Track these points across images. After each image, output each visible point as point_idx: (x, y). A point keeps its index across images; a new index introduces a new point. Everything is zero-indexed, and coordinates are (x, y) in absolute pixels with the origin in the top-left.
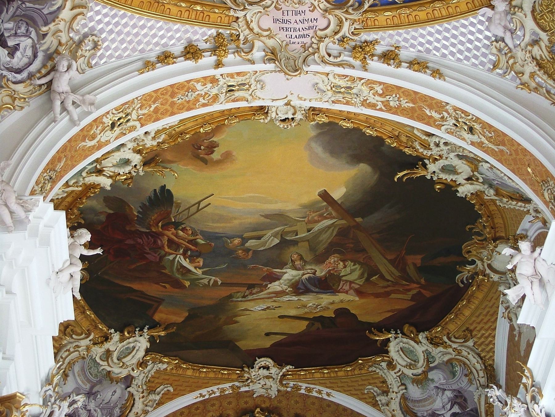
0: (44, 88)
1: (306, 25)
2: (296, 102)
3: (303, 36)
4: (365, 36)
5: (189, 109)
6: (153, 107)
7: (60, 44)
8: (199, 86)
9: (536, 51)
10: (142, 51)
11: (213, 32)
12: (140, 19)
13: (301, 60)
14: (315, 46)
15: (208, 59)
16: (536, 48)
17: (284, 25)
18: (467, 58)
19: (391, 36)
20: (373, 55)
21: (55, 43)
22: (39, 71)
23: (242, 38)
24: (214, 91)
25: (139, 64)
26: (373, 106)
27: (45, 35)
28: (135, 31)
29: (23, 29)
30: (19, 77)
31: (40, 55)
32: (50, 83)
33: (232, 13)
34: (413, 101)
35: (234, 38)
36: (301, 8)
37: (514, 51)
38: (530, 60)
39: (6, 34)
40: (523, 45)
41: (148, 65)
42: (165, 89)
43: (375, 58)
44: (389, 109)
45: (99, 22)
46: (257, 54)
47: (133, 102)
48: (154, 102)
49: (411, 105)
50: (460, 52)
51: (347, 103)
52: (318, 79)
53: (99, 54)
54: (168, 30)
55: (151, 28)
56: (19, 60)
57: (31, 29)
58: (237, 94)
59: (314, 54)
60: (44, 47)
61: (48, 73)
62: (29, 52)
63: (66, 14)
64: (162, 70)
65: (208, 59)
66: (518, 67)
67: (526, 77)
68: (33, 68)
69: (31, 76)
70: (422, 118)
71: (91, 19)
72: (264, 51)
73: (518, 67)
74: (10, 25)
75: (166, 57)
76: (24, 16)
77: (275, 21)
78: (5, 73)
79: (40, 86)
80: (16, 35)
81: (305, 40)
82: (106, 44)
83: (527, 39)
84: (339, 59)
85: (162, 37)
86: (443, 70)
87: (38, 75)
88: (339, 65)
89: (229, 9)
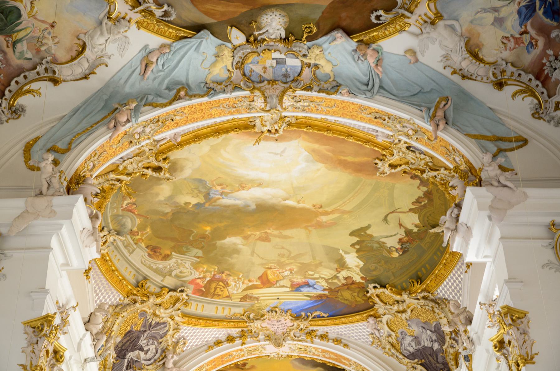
0: (161, 366)
1: (283, 325)
2: (281, 353)
3: (282, 329)
4: (311, 328)
5: (231, 361)
6: (213, 364)
7: (168, 345)
8: (234, 353)
9: (390, 339)
10: (206, 341)
11: (240, 329)
12: (205, 329)
13: (282, 339)
14: (289, 333)
15: (238, 341)
16: (390, 339)
17: (273, 326)
18: (360, 339)
19: (324, 329)
20: (316, 336)
21: (166, 345)
22: (159, 358)
23: (253, 331)
24: (242, 353)
25: (206, 347)
26: (319, 356)
27: (161, 343)
28: (203, 334)
29: (151, 342)
30: (150, 362)
31: (159, 351)
32: (164, 364)
33: (247, 324)
34: (336, 356)
35: (250, 331)
36: (280, 319)
37: (380, 338)
38: (387, 344)
39: (143, 346)
40: (384, 336)
41: (210, 348)
42: (219, 357)
43: (317, 338)
44: (326, 358)
45: (186, 333)
46: (261, 337)
47: (203, 365)
48: (214, 362)
49: (335, 357)
50: (356, 336)
51: (306, 354)
52: (290, 346)
53: (186, 345)
54: (218, 332)
55: (210, 332)
56: (150, 355)
57: (154, 341)
58: (253, 353)
59: (288, 336)
60: (161, 347)
61: (163, 359)
62: (154, 351)
63: (171, 332)
64: (216, 349)
65: (238, 341)
66: (383, 345)
67: (387, 350)
68: (156, 357)
69: (155, 361)
70: (341, 362)
71: (182, 332)
72: (264, 335)
73: (383, 345)
74: (145, 341)
75: (218, 343)
76: (151, 336)
77: (269, 324)
78: (143, 362)
79: (160, 365)
80: (148, 345)
81: (283, 331)
82: (189, 341)
83: (386, 334)
84: (300, 339)
85: (216, 334)
86: (350, 344)
87: (158, 360)
88: (300, 341)
89: (247, 322)
